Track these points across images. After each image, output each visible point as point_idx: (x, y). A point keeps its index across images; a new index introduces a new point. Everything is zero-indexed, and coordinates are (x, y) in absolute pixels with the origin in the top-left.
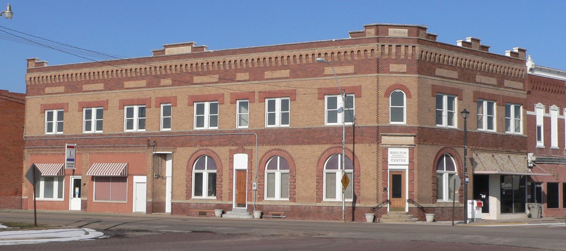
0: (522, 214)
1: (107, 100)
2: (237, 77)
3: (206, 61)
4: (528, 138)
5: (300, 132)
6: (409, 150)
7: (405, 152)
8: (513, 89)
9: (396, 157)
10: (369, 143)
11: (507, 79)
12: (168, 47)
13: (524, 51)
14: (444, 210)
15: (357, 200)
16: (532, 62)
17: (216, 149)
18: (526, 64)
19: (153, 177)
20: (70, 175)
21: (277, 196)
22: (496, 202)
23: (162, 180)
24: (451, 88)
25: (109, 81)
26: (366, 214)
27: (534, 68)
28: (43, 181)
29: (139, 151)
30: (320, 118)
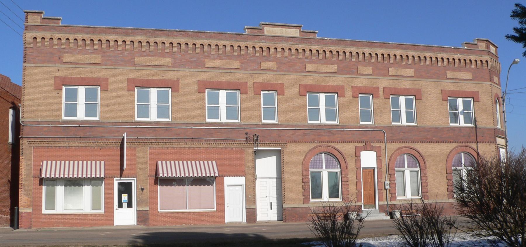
1: (178, 80)
17: (339, 146)
29: (232, 146)
30: (446, 118)
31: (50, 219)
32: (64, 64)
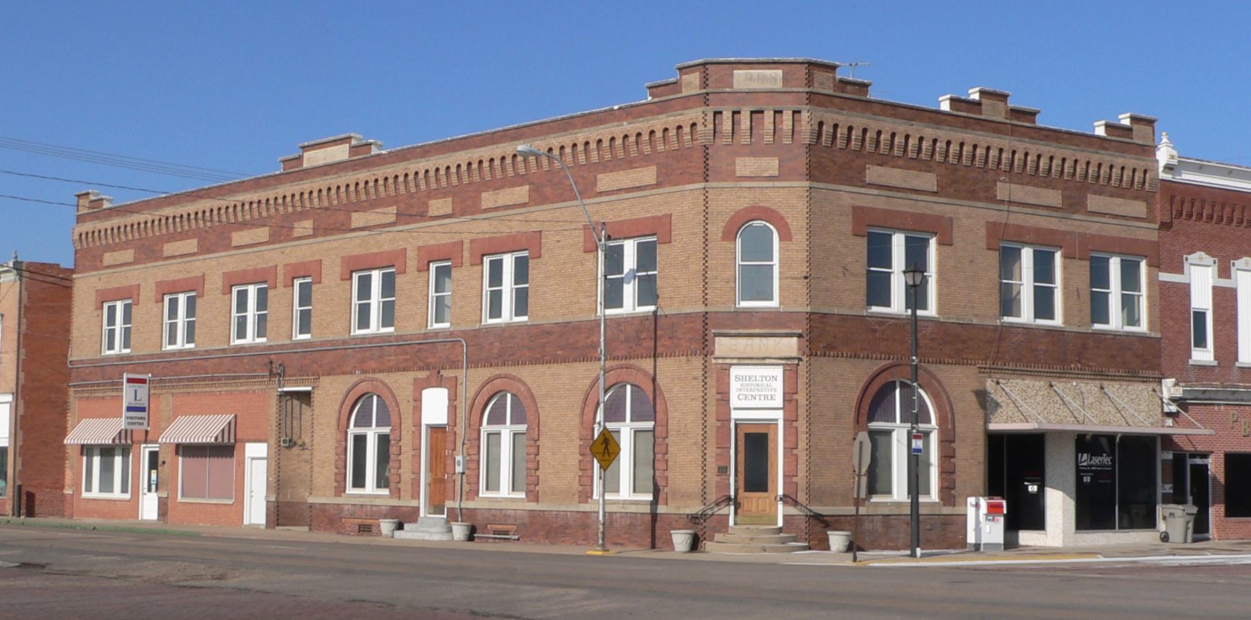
0: (1149, 533)
2: (429, 209)
3: (374, 175)
4: (1163, 341)
5: (549, 333)
6: (784, 370)
7: (773, 377)
8: (1115, 216)
9: (751, 390)
10: (687, 355)
11: (1095, 193)
12: (308, 148)
13: (1150, 122)
14: (893, 522)
15: (662, 496)
16: (1173, 148)
17: (391, 379)
18: (1155, 155)
19: (279, 446)
20: (140, 443)
21: (505, 490)
22: (1061, 502)
23: (302, 452)
24: (913, 215)
25: (206, 232)
26: (672, 532)
27: (1176, 164)
28: (98, 456)
30: (589, 296)
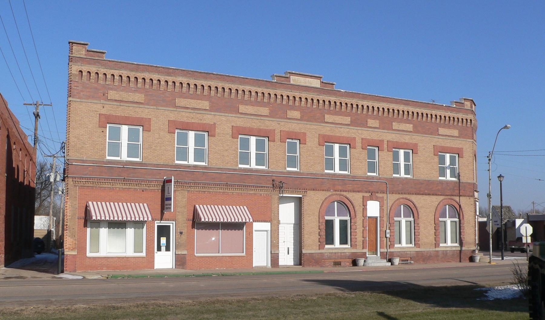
5: (422, 184)
17: (350, 195)
29: (261, 193)
30: (436, 172)
31: (94, 262)
32: (109, 101)
